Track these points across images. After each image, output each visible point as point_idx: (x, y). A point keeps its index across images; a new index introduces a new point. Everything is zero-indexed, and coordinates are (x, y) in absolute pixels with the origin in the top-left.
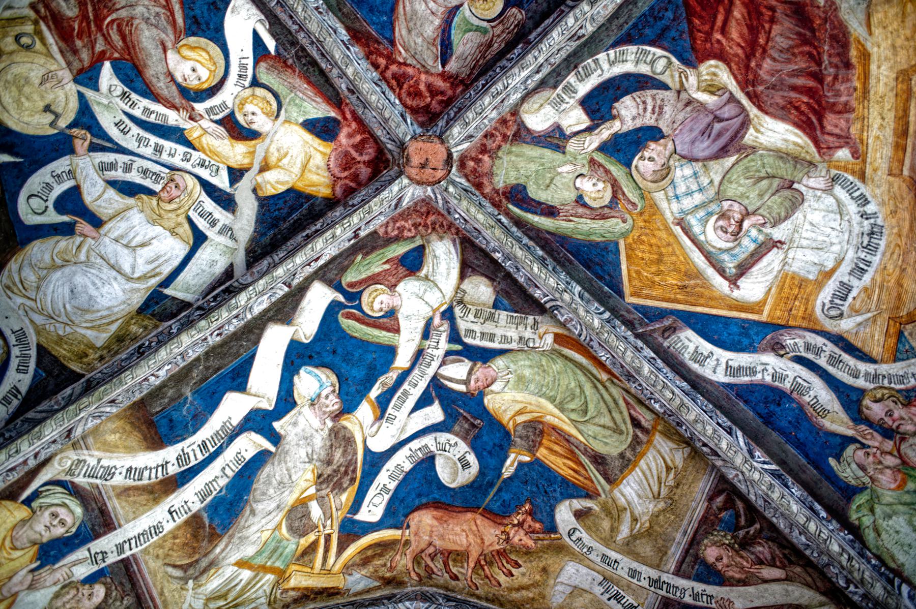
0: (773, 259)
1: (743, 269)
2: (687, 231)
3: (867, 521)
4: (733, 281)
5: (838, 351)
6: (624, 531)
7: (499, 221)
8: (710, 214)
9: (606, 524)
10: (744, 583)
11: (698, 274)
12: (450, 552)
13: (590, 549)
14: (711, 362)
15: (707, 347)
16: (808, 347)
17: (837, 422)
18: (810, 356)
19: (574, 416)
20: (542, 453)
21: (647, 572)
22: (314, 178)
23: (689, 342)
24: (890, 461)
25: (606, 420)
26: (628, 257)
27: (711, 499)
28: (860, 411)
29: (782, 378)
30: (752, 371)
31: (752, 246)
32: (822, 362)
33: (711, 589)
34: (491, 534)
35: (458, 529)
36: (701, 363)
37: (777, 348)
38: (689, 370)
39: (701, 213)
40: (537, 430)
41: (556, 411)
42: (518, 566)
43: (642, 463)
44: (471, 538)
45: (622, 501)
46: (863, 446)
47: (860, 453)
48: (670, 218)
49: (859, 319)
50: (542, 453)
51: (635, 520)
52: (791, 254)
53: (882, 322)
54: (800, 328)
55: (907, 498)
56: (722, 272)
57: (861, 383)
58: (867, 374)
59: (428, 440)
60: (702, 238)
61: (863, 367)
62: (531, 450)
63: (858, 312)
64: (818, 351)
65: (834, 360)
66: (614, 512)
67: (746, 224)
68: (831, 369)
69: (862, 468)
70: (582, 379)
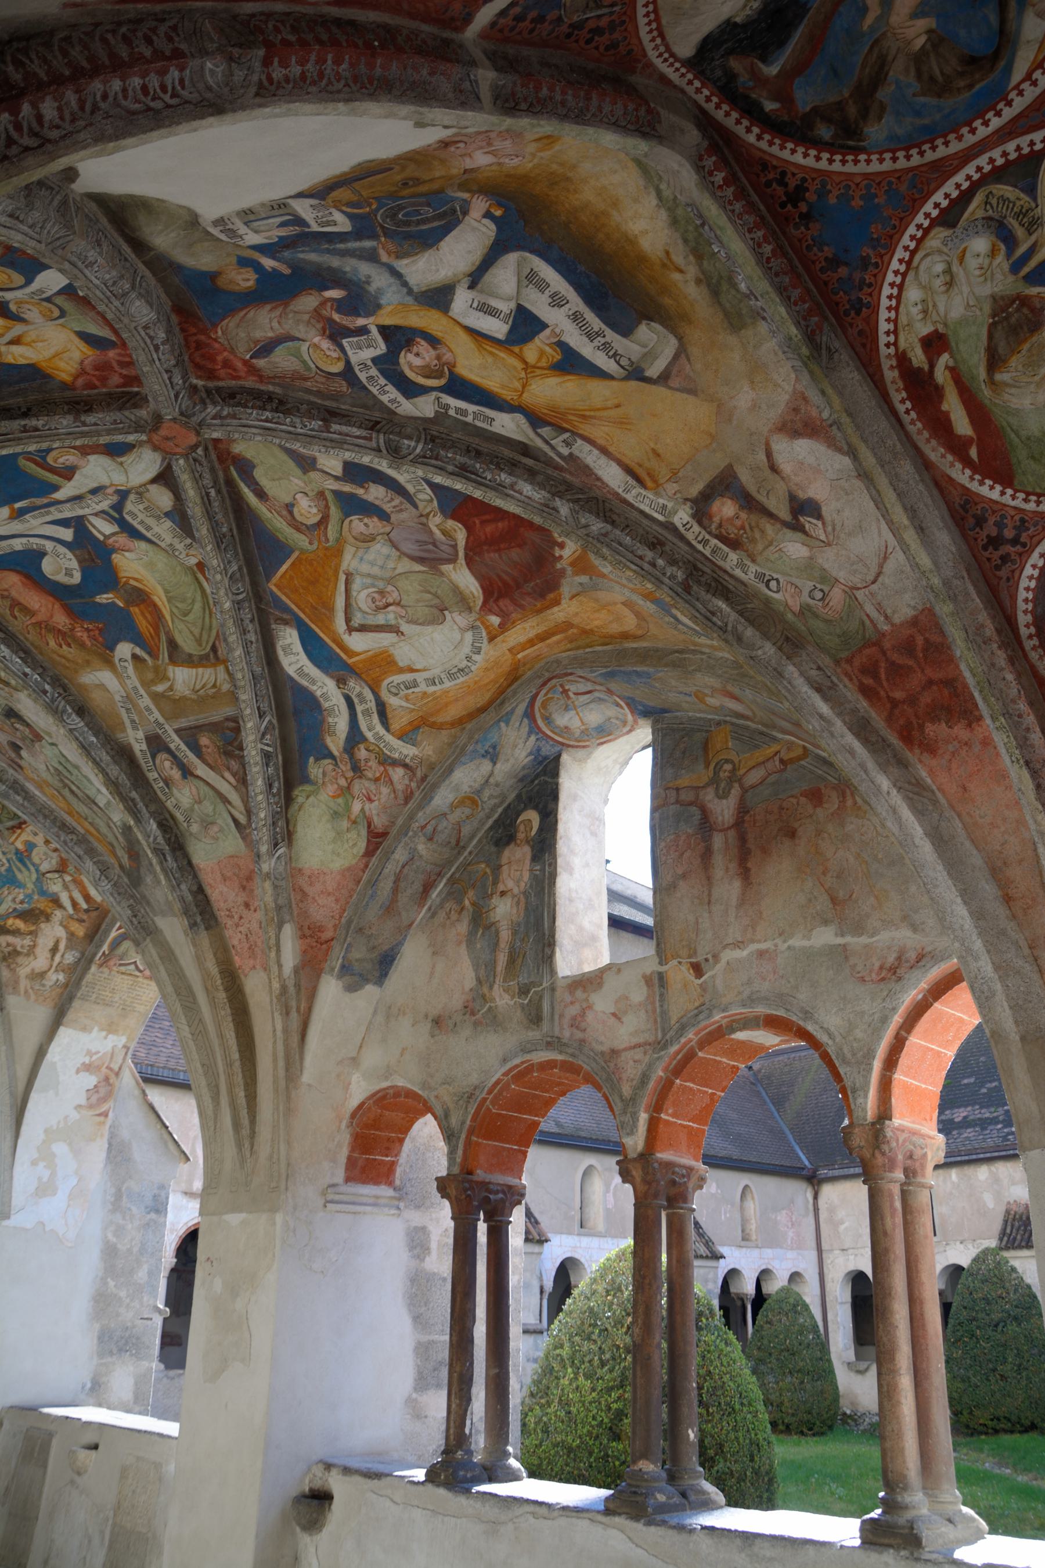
0: (385, 640)
1: (363, 628)
2: (347, 583)
3: (300, 800)
4: (350, 630)
5: (374, 709)
6: (160, 688)
7: (208, 494)
8: (373, 586)
9: (150, 676)
10: (211, 767)
11: (332, 609)
12: (19, 604)
13: (129, 677)
14: (293, 658)
15: (298, 647)
16: (359, 695)
17: (336, 743)
18: (356, 700)
19: (175, 610)
20: (135, 610)
21: (157, 714)
22: (62, 365)
23: (289, 638)
24: (343, 782)
25: (197, 631)
26: (293, 564)
27: (227, 719)
28: (353, 748)
29: (327, 699)
30: (313, 682)
31: (382, 622)
32: (359, 709)
33: (189, 753)
34: (61, 619)
35: (36, 599)
36: (286, 654)
37: (341, 682)
38: (275, 652)
39: (369, 581)
40: (140, 596)
41: (164, 599)
42: (69, 645)
43: (200, 670)
44: (43, 610)
45: (171, 675)
46: (336, 764)
47: (331, 767)
48: (344, 566)
49: (404, 704)
50: (135, 610)
51: (171, 688)
52: (401, 644)
53: (413, 716)
54: (366, 682)
55: (332, 804)
56: (348, 620)
57: (369, 735)
58: (377, 733)
59: (49, 545)
60: (354, 594)
61: (380, 729)
62: (128, 603)
63: (407, 700)
64: (363, 701)
65: (367, 713)
66: (161, 676)
67: (391, 608)
68: (360, 716)
69: (324, 774)
70: (199, 598)
